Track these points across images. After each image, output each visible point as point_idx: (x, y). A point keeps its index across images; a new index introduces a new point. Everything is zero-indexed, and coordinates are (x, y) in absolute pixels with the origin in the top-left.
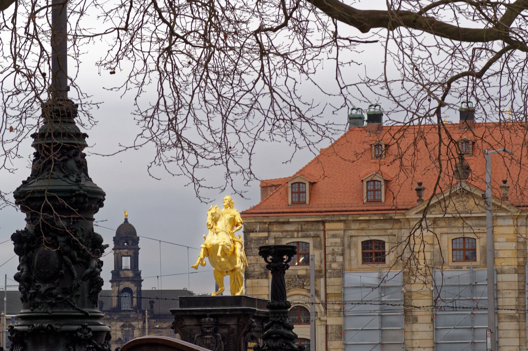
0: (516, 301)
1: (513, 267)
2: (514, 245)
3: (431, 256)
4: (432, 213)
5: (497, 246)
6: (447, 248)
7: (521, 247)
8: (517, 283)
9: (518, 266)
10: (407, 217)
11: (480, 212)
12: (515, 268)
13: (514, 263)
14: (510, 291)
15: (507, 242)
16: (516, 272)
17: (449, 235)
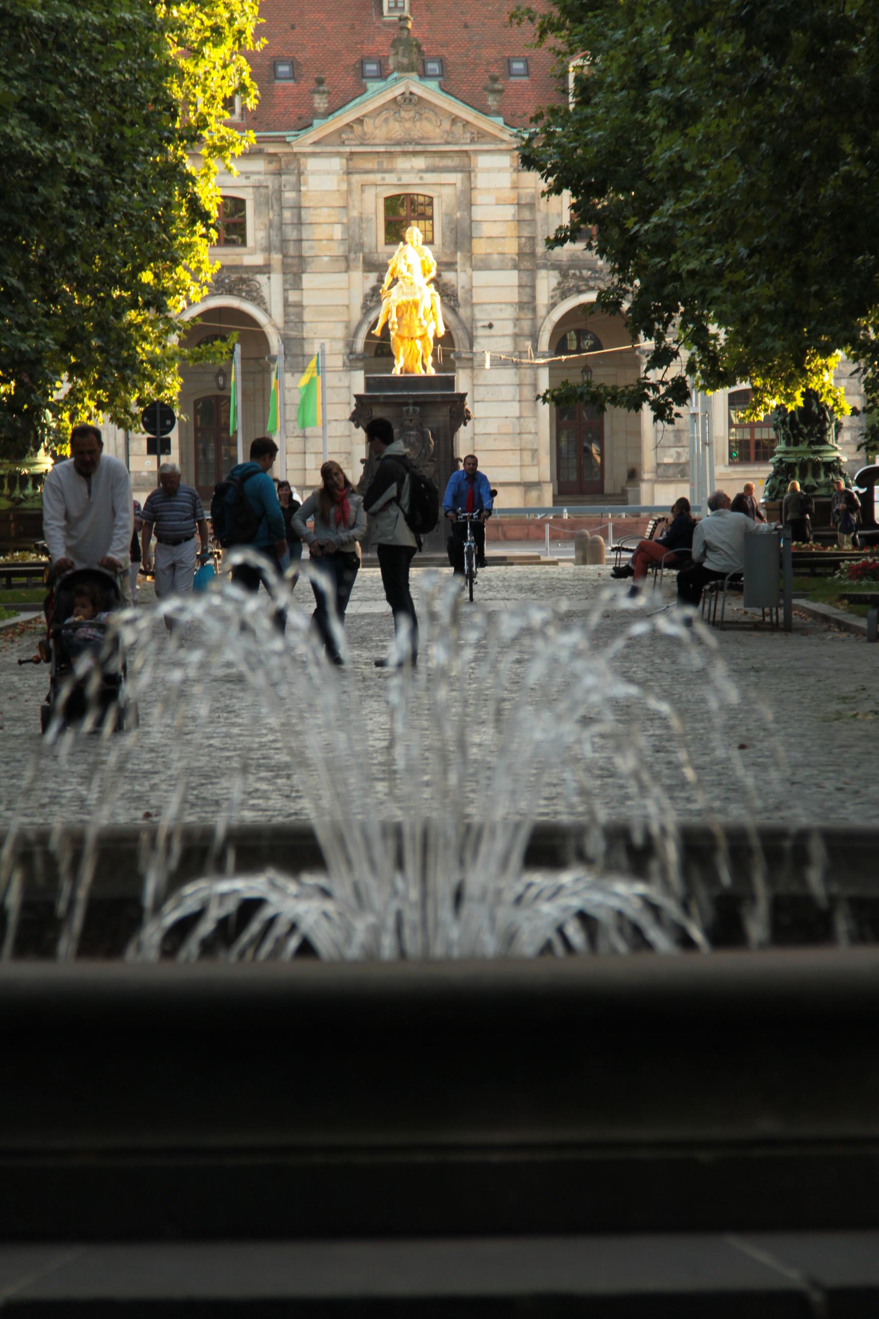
0: (515, 325)
1: (509, 256)
2: (509, 212)
3: (343, 233)
4: (347, 142)
5: (478, 213)
6: (374, 217)
7: (526, 215)
8: (516, 290)
9: (519, 254)
10: (295, 150)
11: (442, 141)
12: (514, 260)
13: (511, 248)
14: (503, 306)
15: (497, 204)
16: (516, 267)
17: (379, 189)
